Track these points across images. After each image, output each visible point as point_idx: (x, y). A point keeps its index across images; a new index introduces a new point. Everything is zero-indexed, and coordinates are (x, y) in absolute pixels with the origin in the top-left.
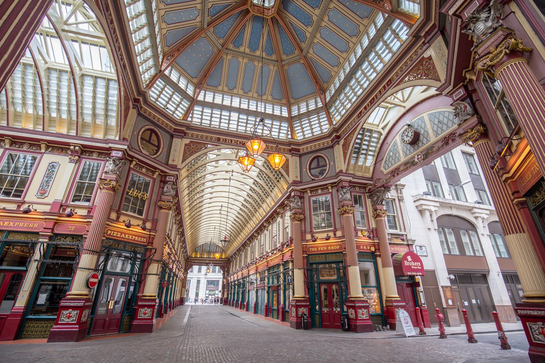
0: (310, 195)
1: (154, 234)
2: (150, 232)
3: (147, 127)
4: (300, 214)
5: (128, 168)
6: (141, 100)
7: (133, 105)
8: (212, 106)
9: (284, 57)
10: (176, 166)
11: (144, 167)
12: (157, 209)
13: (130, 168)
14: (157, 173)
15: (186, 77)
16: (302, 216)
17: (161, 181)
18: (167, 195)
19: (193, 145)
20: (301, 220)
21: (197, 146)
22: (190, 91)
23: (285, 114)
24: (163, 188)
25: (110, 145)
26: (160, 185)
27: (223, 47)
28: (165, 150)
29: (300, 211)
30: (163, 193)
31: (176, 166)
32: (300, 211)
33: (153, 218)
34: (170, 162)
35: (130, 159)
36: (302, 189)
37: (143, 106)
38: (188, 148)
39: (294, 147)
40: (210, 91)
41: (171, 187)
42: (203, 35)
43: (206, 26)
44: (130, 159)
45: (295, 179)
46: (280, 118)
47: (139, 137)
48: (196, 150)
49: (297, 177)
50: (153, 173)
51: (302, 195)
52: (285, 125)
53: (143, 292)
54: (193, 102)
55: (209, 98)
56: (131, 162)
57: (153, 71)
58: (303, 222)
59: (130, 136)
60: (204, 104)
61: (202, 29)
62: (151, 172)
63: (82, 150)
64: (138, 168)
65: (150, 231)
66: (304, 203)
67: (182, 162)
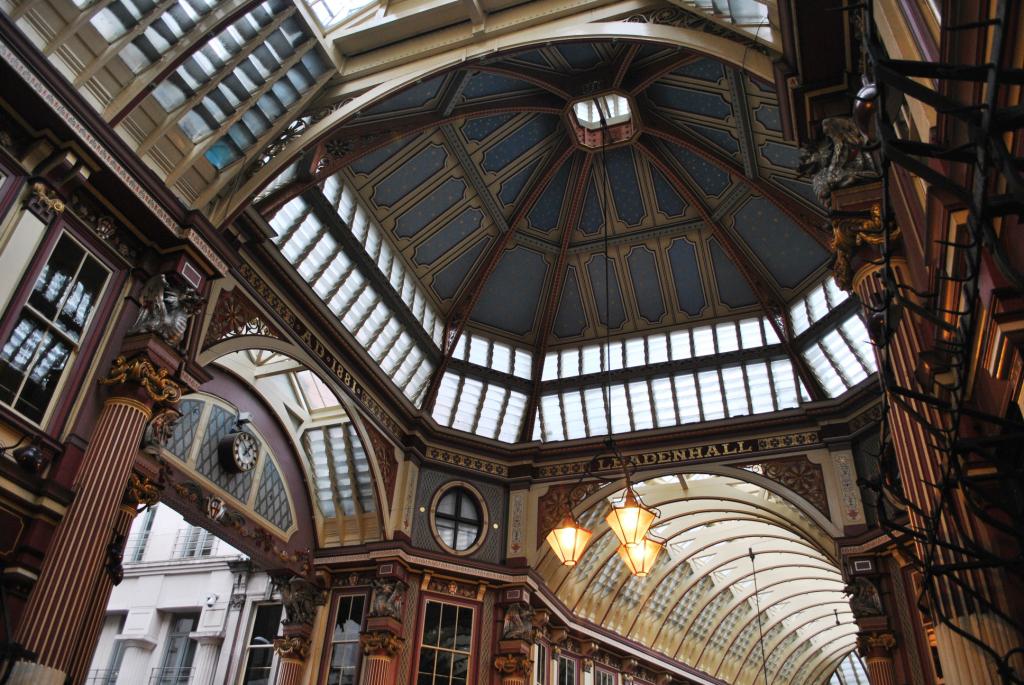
0: (903, 563)
3: (446, 487)
4: (879, 634)
5: (416, 595)
6: (418, 435)
7: (405, 452)
8: (582, 383)
9: (713, 201)
10: (524, 560)
11: (450, 581)
12: (496, 678)
13: (422, 594)
14: (483, 589)
15: (504, 341)
16: (886, 638)
17: (497, 606)
18: (512, 639)
20: (888, 653)
22: (523, 367)
23: (773, 338)
24: (503, 622)
25: (374, 555)
26: (495, 614)
27: (560, 247)
28: (496, 526)
31: (524, 560)
32: (882, 621)
35: (419, 572)
36: (875, 549)
37: (427, 443)
38: (548, 506)
39: (826, 423)
40: (569, 346)
41: (517, 616)
42: (509, 245)
43: (504, 227)
44: (419, 572)
45: (851, 522)
46: (765, 354)
47: (432, 515)
49: (853, 514)
50: (475, 589)
51: (882, 570)
52: (784, 370)
54: (534, 390)
55: (570, 370)
56: (421, 578)
57: (426, 369)
58: (898, 656)
59: (410, 522)
60: (561, 386)
61: (502, 237)
62: (470, 590)
63: (331, 574)
64: (440, 587)
66: (891, 593)
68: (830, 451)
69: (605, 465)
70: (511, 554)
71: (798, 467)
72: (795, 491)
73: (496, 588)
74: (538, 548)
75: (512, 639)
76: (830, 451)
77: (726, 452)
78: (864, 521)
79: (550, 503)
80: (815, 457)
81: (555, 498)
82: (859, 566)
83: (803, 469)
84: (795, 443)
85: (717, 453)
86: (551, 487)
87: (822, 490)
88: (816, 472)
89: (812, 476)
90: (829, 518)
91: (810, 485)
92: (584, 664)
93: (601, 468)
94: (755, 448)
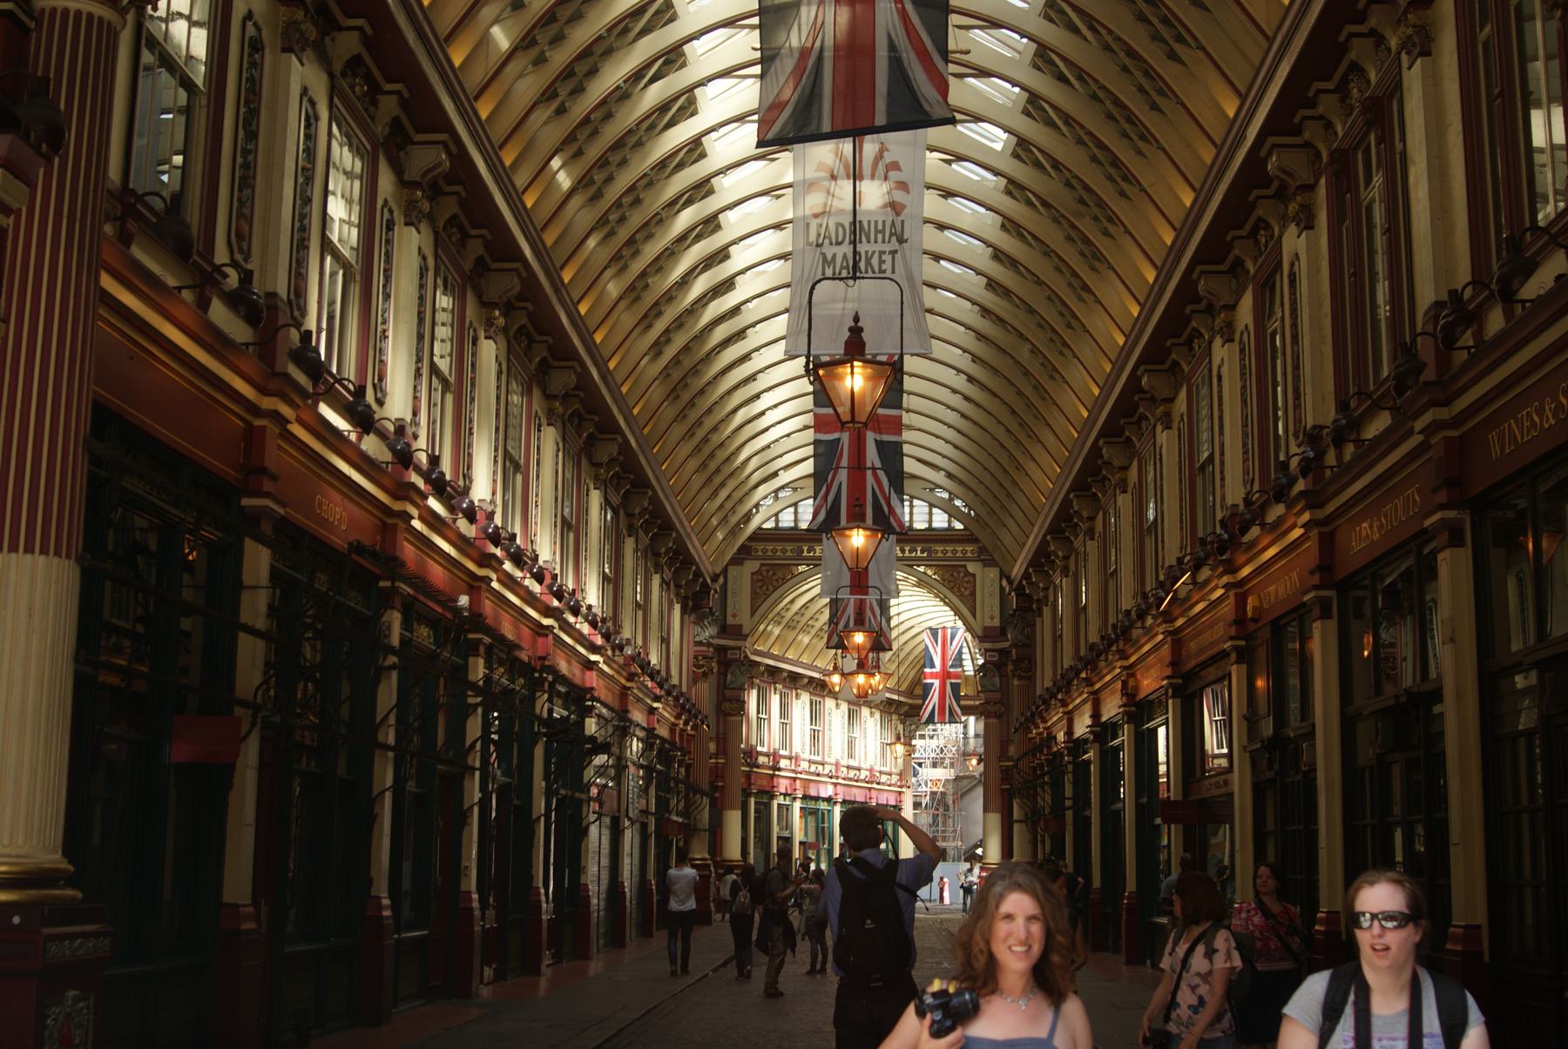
1: (722, 761)
2: (716, 758)
4: (995, 703)
10: (740, 626)
18: (734, 689)
19: (768, 571)
20: (999, 716)
21: (774, 574)
29: (998, 695)
30: (725, 687)
31: (740, 626)
32: (998, 695)
33: (718, 734)
34: (730, 621)
38: (758, 581)
45: (988, 623)
48: (775, 583)
49: (992, 618)
53: (721, 855)
65: (716, 756)
67: (752, 615)
68: (984, 566)
69: (809, 552)
70: (730, 621)
71: (959, 573)
72: (953, 593)
73: (721, 650)
74: (752, 616)
75: (734, 689)
76: (984, 566)
77: (907, 554)
78: (998, 624)
79: (760, 578)
80: (971, 567)
81: (765, 573)
82: (990, 656)
83: (962, 574)
84: (959, 554)
85: (900, 555)
86: (762, 565)
87: (973, 594)
88: (971, 579)
89: (967, 582)
90: (975, 617)
91: (966, 588)
92: (752, 683)
93: (805, 554)
94: (930, 551)
